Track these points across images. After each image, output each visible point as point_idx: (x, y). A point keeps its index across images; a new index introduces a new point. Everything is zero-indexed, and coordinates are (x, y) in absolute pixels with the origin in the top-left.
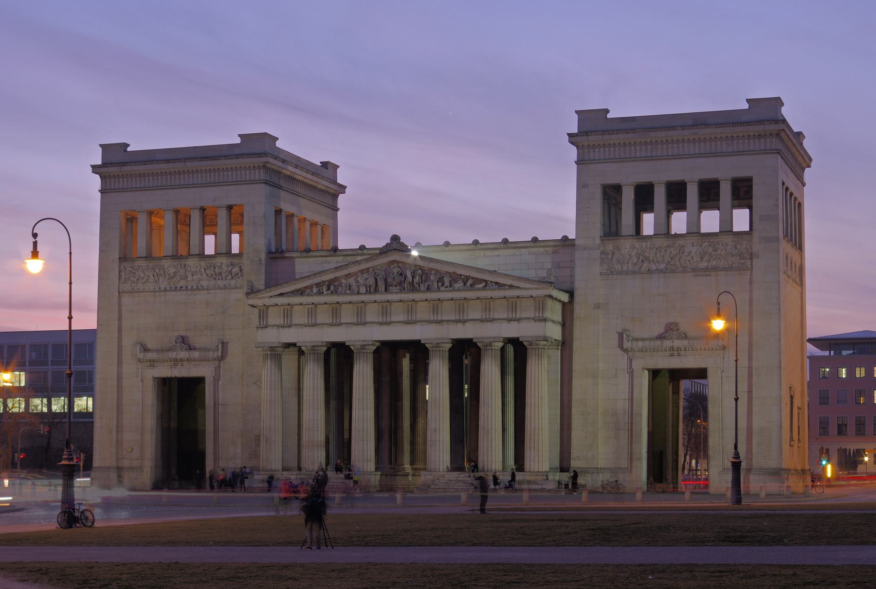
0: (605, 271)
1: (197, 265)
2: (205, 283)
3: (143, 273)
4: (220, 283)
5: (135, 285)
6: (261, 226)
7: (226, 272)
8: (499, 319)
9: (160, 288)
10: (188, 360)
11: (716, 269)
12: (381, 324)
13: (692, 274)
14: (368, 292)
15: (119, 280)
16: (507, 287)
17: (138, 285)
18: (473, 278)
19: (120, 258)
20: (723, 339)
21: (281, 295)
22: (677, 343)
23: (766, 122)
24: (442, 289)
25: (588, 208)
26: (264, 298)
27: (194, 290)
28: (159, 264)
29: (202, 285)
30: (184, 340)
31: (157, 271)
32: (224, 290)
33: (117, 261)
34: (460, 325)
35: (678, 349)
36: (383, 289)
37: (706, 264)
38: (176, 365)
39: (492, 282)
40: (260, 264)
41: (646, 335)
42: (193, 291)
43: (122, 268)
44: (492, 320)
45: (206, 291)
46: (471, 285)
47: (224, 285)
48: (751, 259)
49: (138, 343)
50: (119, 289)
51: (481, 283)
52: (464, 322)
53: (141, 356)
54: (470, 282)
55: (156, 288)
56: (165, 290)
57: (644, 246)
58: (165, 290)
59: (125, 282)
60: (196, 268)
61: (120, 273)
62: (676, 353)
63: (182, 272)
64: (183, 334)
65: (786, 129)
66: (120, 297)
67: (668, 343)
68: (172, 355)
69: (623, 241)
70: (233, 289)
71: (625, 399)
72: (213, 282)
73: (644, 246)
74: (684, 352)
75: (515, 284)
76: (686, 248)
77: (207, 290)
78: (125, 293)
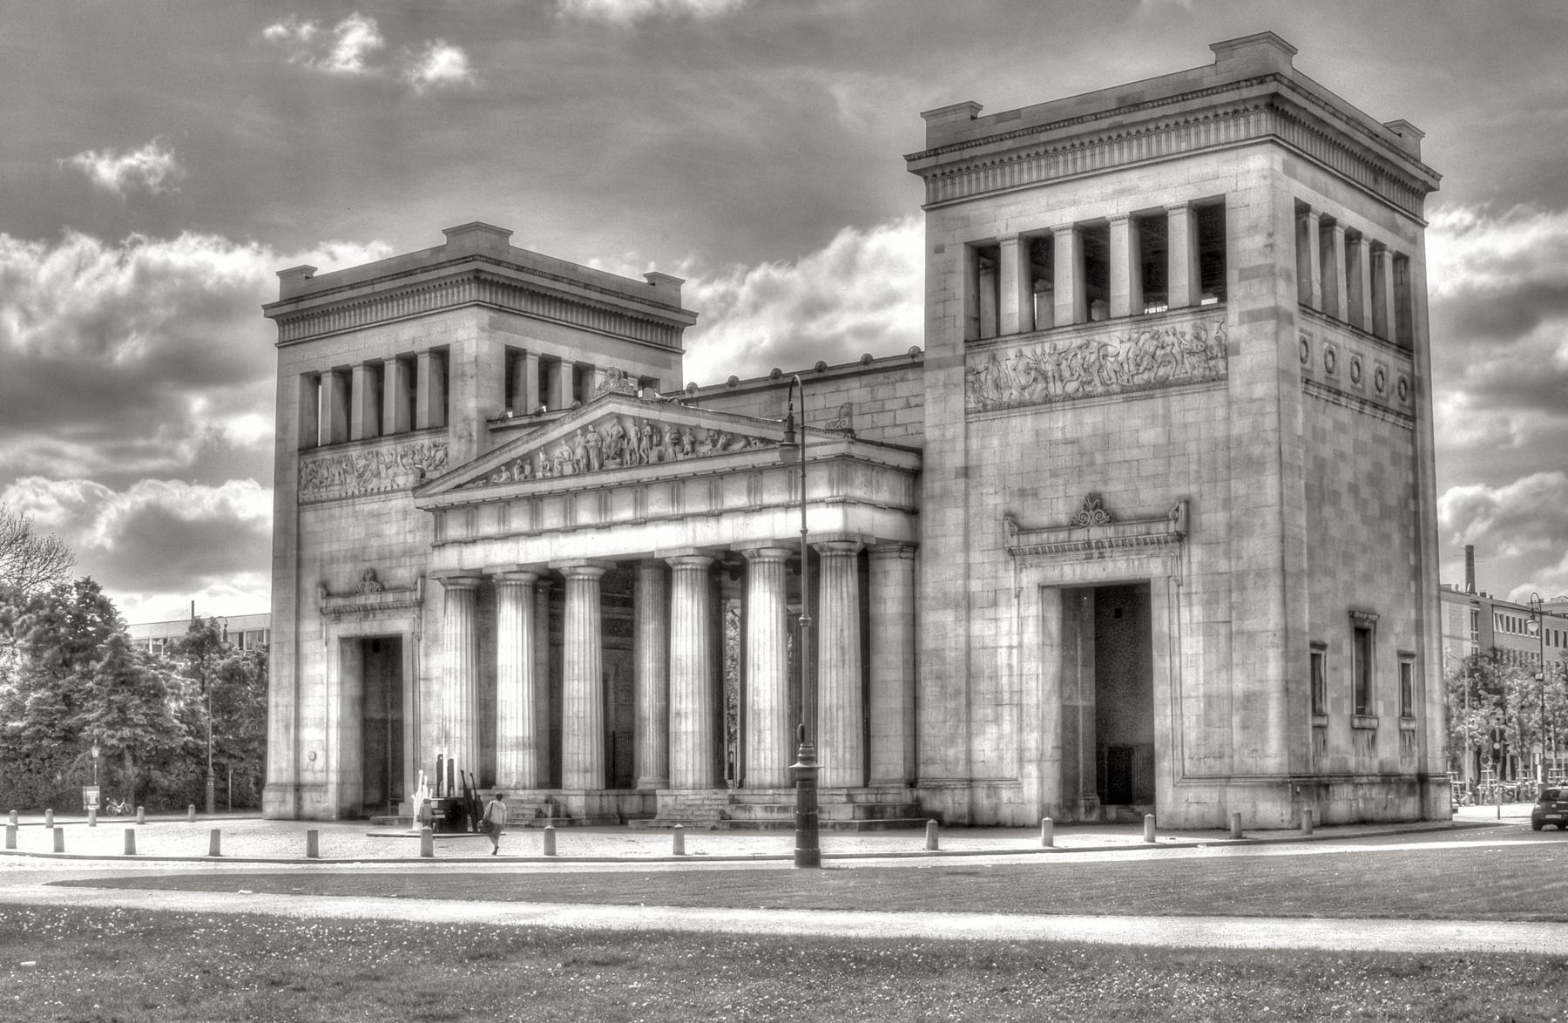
0: (973, 405)
8: (769, 507)
11: (1164, 384)
12: (599, 528)
13: (1121, 396)
14: (576, 474)
15: (299, 483)
18: (726, 434)
20: (1176, 520)
21: (459, 487)
23: (1243, 84)
26: (435, 494)
30: (374, 576)
33: (296, 454)
34: (712, 523)
35: (1100, 545)
37: (1146, 376)
38: (366, 616)
39: (755, 438)
41: (1044, 520)
44: (762, 509)
46: (726, 446)
48: (1225, 357)
52: (717, 515)
53: (323, 604)
54: (722, 440)
56: (353, 496)
57: (1039, 351)
58: (353, 496)
59: (306, 487)
62: (1095, 553)
63: (373, 466)
64: (375, 565)
65: (1286, 93)
67: (1079, 535)
68: (360, 601)
69: (1003, 346)
71: (1010, 647)
73: (1039, 351)
74: (1109, 550)
76: (1110, 348)
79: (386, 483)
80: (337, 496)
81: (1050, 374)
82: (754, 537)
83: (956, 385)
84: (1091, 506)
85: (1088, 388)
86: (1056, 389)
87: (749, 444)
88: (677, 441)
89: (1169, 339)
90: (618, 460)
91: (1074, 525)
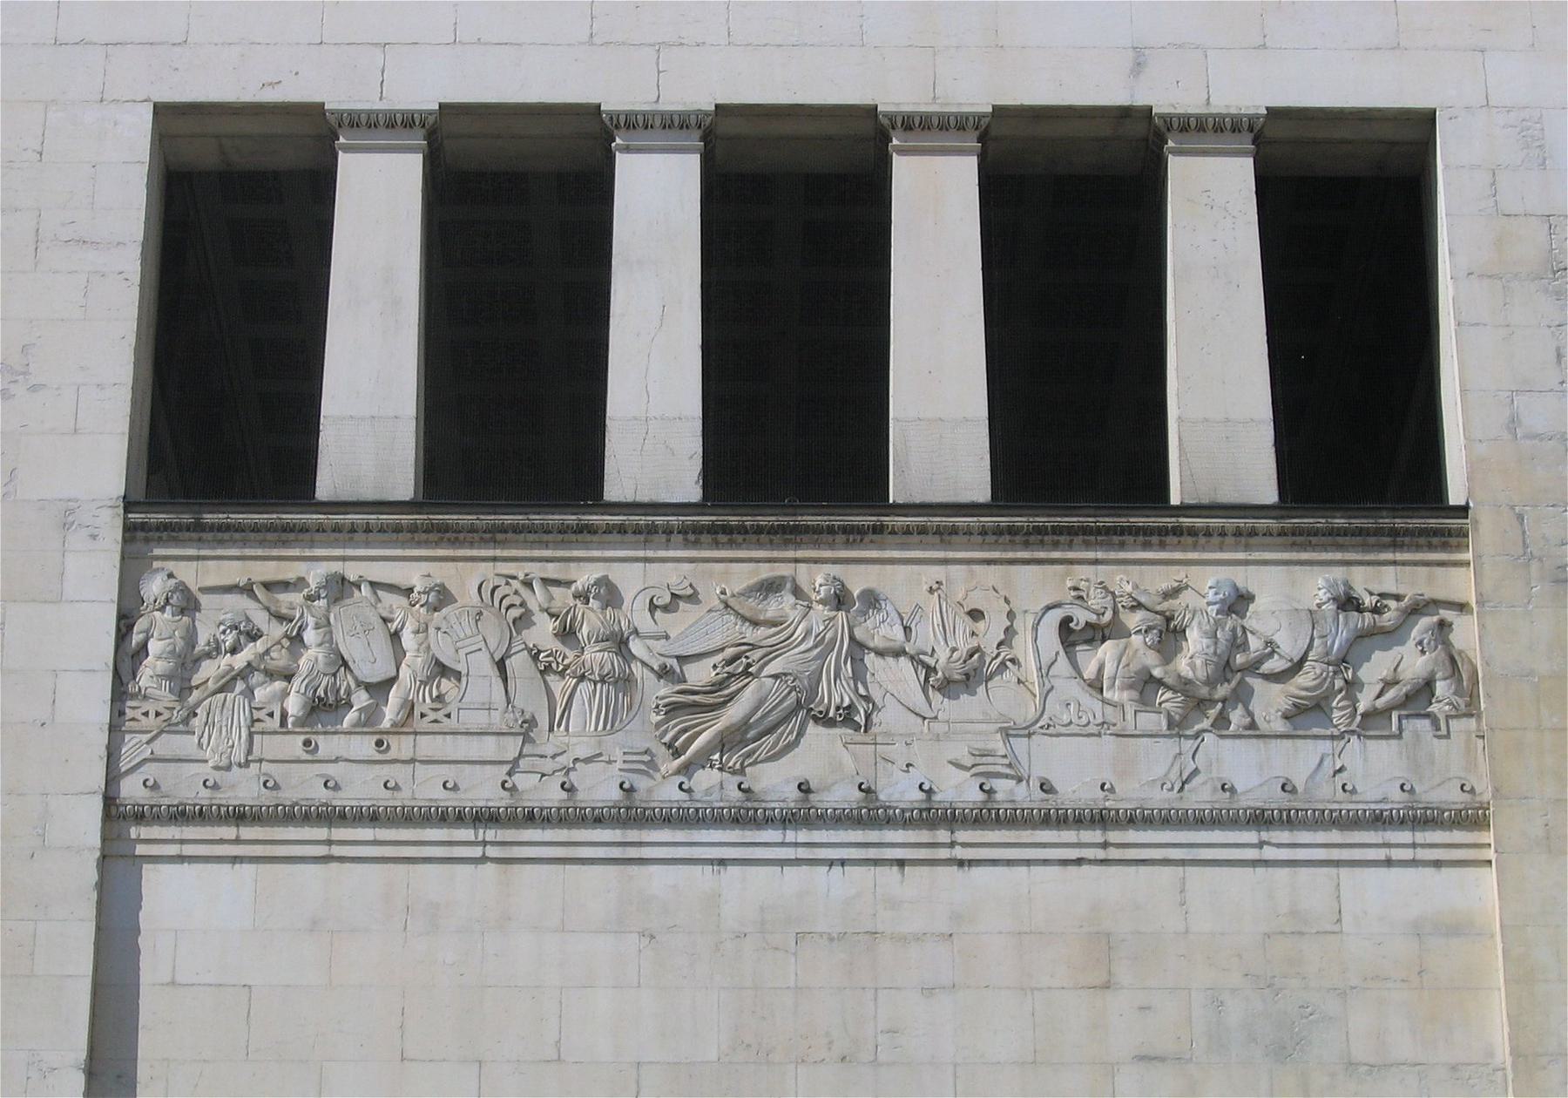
1: (976, 601)
5: (293, 745)
7: (1298, 666)
9: (568, 788)
15: (121, 689)
17: (328, 745)
19: (129, 505)
27: (952, 819)
28: (552, 571)
29: (1038, 772)
42: (943, 835)
43: (154, 587)
45: (1095, 836)
50: (113, 777)
55: (521, 781)
60: (964, 624)
70: (1379, 820)
77: (1101, 819)
78: (180, 816)
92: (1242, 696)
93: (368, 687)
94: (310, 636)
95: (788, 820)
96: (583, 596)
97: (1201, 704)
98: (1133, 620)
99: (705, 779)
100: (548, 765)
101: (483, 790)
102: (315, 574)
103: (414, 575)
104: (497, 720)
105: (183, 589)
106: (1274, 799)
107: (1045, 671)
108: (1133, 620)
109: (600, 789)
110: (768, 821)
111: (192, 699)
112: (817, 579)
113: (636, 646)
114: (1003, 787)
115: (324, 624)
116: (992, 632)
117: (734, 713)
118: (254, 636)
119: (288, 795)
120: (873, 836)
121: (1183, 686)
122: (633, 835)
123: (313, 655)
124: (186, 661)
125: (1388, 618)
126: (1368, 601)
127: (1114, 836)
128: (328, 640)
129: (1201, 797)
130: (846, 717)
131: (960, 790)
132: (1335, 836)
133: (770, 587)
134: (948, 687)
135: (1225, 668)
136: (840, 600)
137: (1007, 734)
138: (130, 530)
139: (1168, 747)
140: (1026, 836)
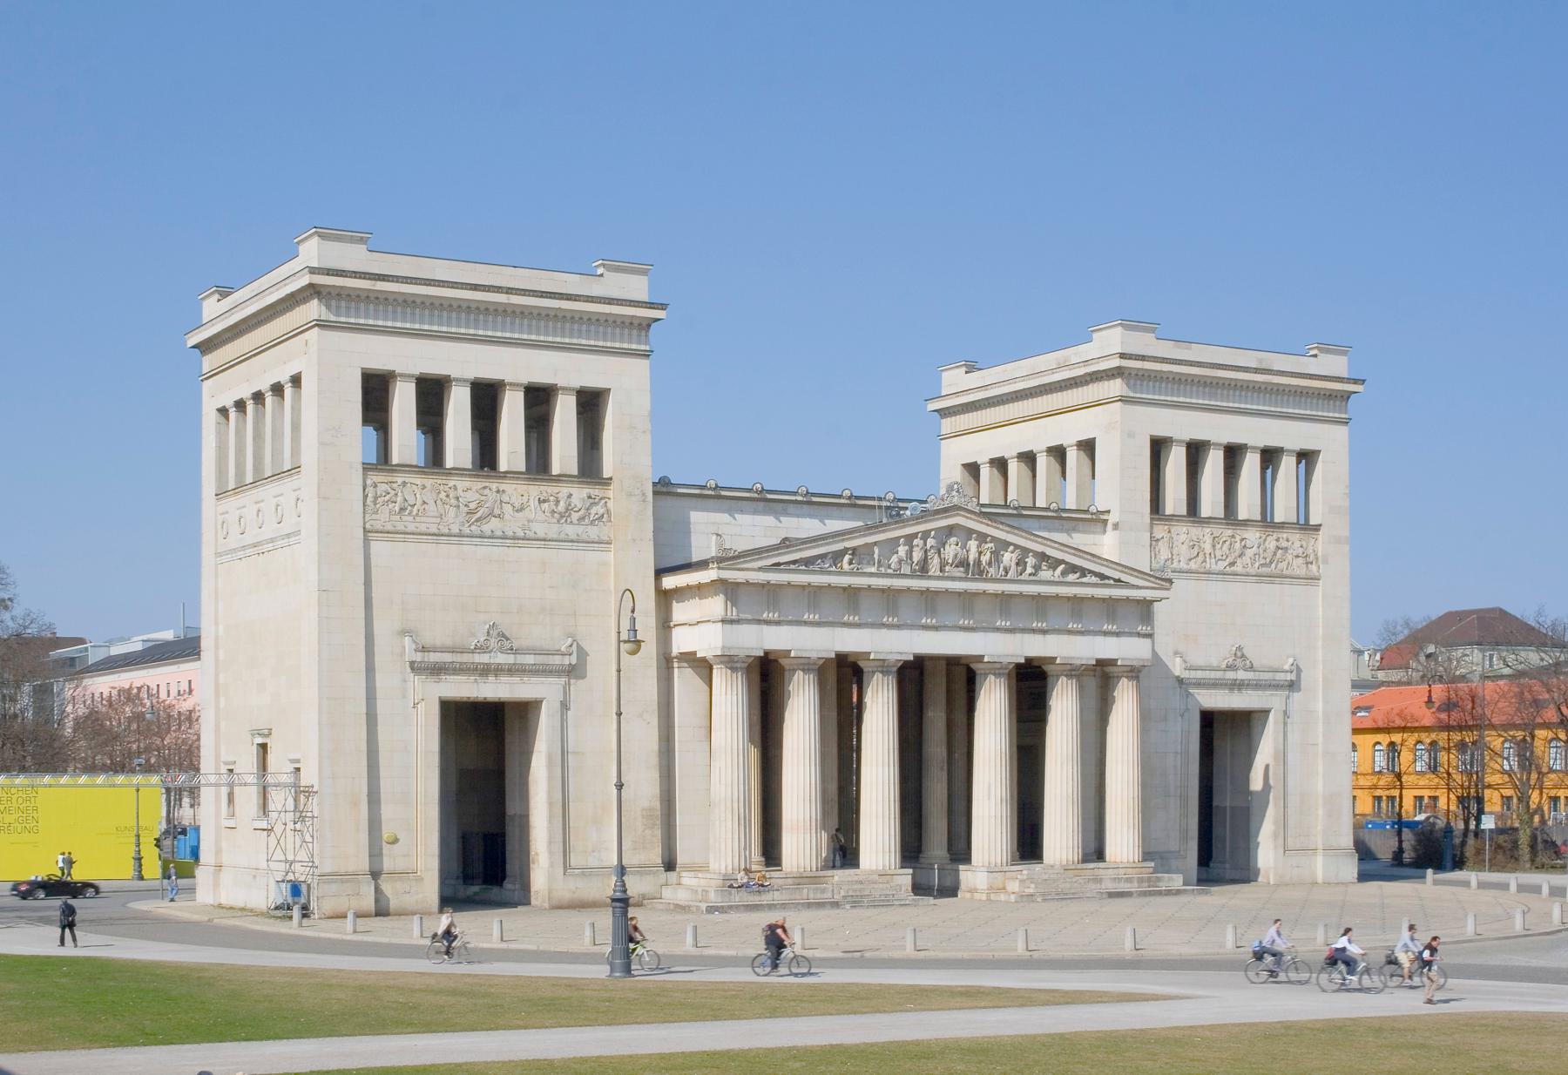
1: (522, 493)
2: (540, 530)
3: (413, 496)
4: (571, 531)
6: (644, 432)
10: (509, 670)
13: (1254, 578)
16: (1112, 582)
17: (404, 518)
18: (1066, 563)
22: (1241, 675)
24: (1023, 577)
25: (1135, 468)
28: (444, 482)
31: (443, 495)
32: (576, 544)
33: (360, 468)
36: (938, 573)
39: (1090, 572)
40: (644, 501)
43: (369, 482)
45: (543, 543)
47: (578, 535)
49: (404, 632)
50: (364, 523)
51: (1076, 573)
56: (460, 535)
61: (364, 490)
66: (366, 541)
70: (593, 542)
72: (555, 528)
75: (1124, 578)
77: (544, 540)
79: (512, 524)
80: (436, 531)
81: (1208, 552)
82: (1078, 656)
83: (1144, 546)
84: (1239, 654)
85: (1232, 568)
86: (1211, 565)
87: (1084, 575)
88: (1021, 563)
89: (1284, 544)
90: (962, 569)
91: (1230, 667)
92: (570, 515)
93: (411, 506)
94: (399, 494)
95: (489, 537)
96: (450, 488)
97: (562, 517)
98: (552, 498)
99: (473, 528)
100: (445, 524)
101: (434, 529)
102: (400, 480)
103: (418, 481)
104: (436, 514)
105: (374, 482)
106: (573, 537)
107: (535, 509)
108: (552, 498)
109: (455, 530)
110: (486, 538)
111: (378, 506)
112: (494, 486)
113: (460, 499)
114: (527, 532)
115: (402, 492)
116: (525, 498)
117: (479, 515)
118: (389, 493)
119: (398, 528)
120: (503, 541)
121: (560, 513)
122: (461, 539)
123: (399, 499)
124: (376, 498)
125: (596, 501)
126: (593, 497)
127: (547, 543)
128: (403, 496)
129: (562, 536)
130: (499, 516)
131: (520, 534)
132: (585, 545)
133: (485, 488)
134: (517, 511)
135: (567, 510)
136: (498, 492)
137: (528, 521)
138: (364, 468)
139: (557, 525)
140: (531, 542)
